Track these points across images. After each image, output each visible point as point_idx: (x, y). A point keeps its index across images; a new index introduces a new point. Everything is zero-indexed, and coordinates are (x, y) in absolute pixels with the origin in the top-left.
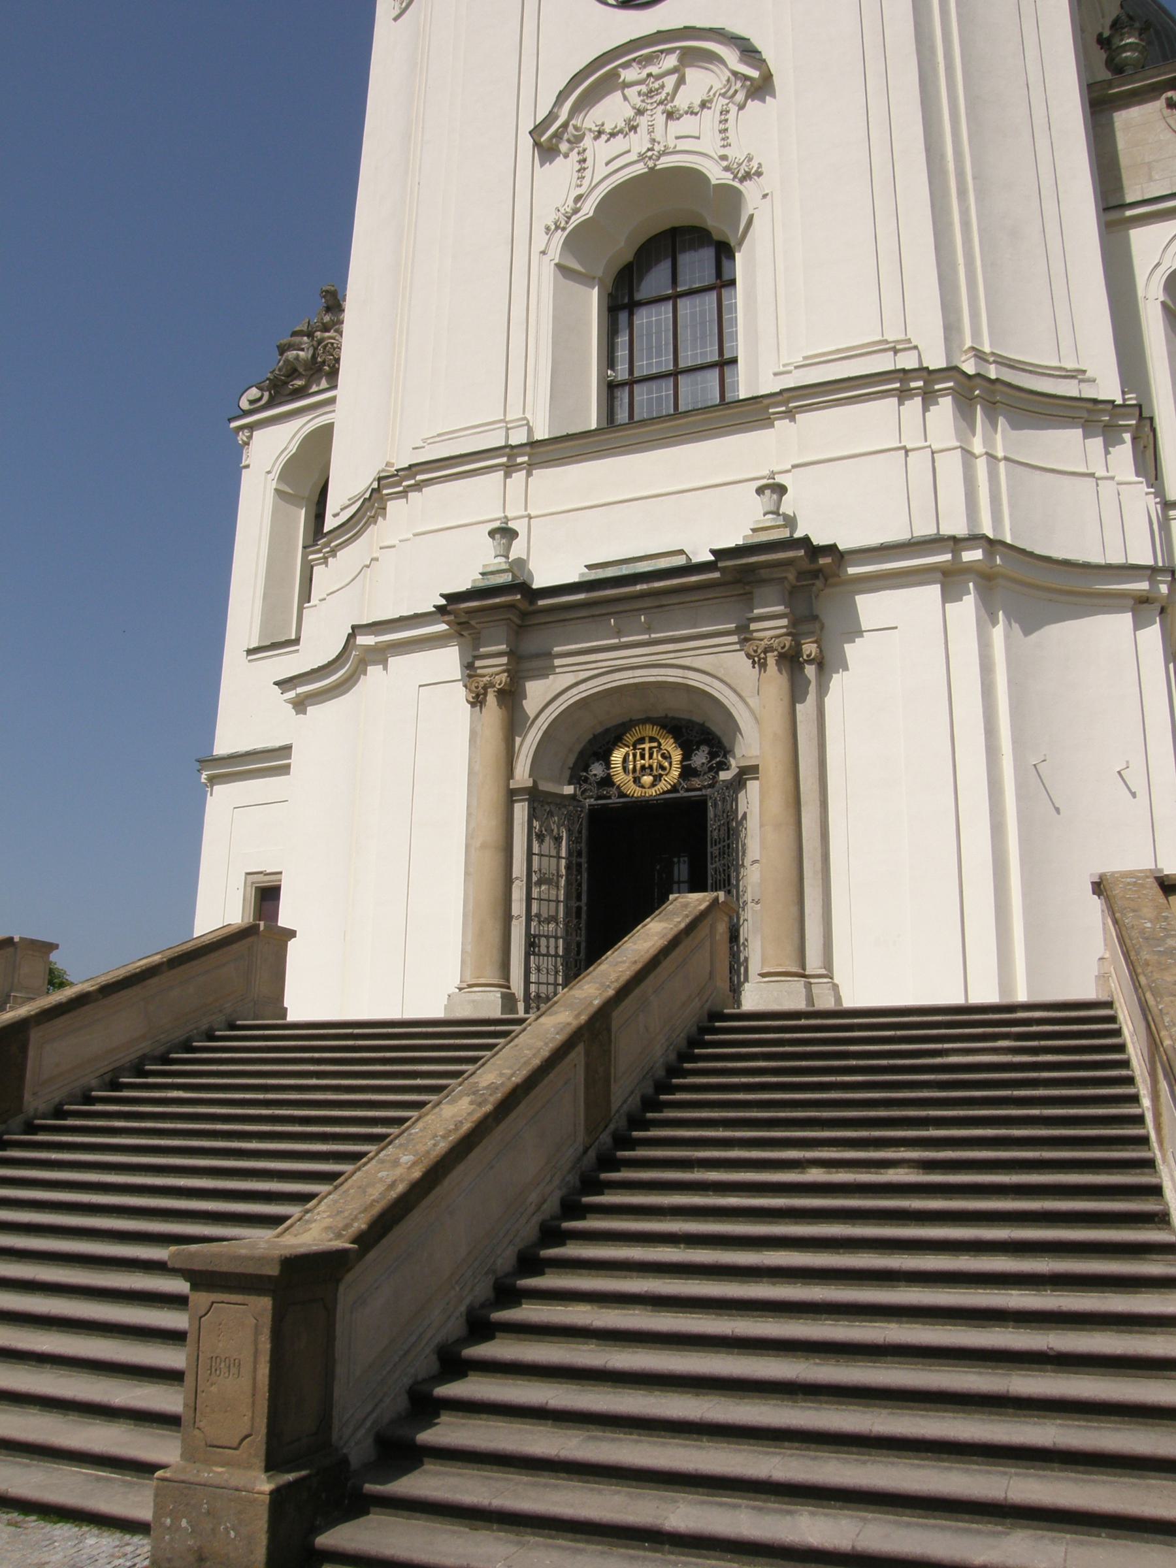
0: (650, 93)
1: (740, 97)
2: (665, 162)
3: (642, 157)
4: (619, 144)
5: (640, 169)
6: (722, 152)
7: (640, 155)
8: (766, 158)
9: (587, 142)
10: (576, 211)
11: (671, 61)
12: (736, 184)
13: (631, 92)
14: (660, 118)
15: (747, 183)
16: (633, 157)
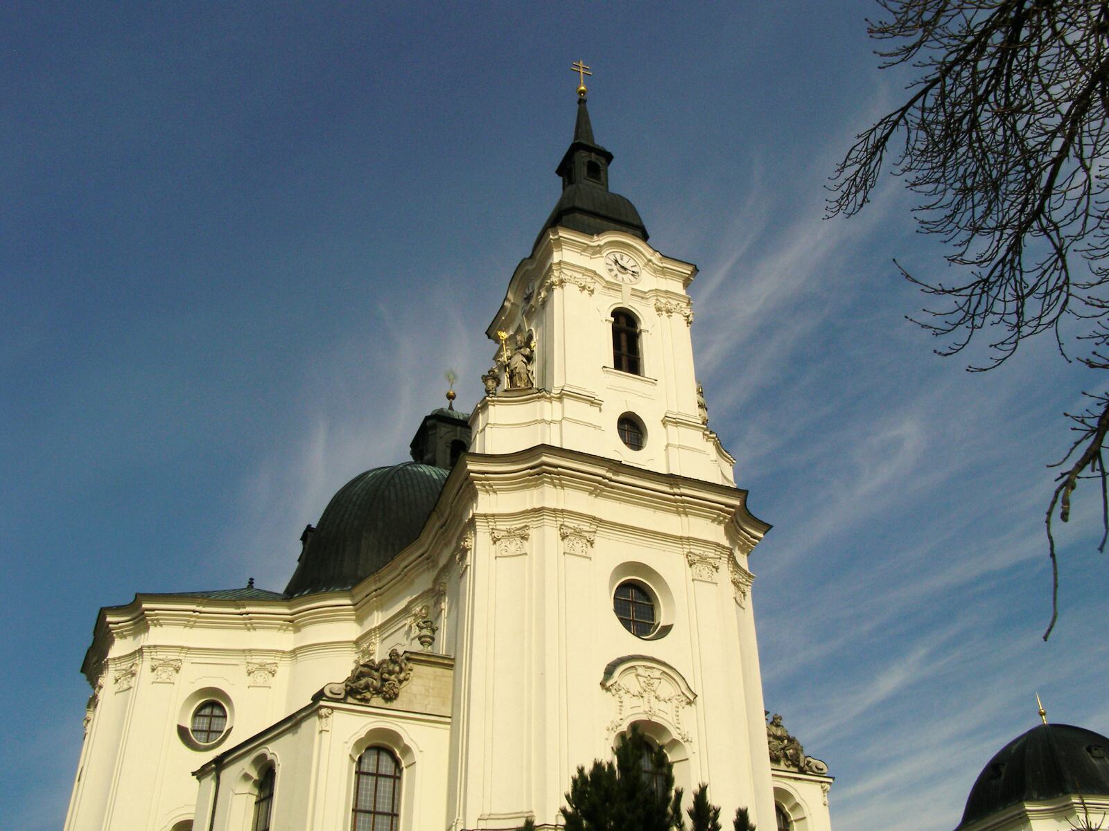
0: (649, 685)
1: (684, 704)
2: (654, 719)
3: (646, 713)
4: (636, 701)
5: (644, 717)
6: (678, 726)
7: (645, 711)
8: (693, 735)
9: (622, 693)
10: (620, 725)
11: (657, 674)
12: (682, 741)
13: (641, 679)
14: (653, 699)
15: (687, 743)
16: (641, 711)
